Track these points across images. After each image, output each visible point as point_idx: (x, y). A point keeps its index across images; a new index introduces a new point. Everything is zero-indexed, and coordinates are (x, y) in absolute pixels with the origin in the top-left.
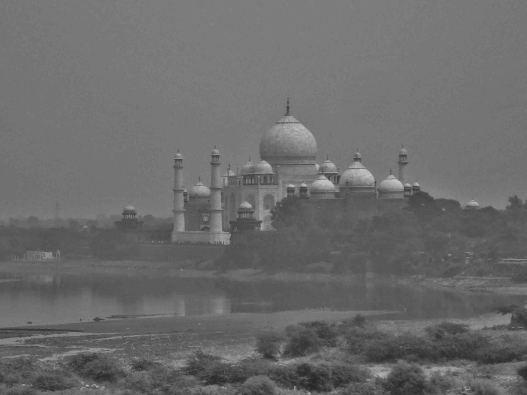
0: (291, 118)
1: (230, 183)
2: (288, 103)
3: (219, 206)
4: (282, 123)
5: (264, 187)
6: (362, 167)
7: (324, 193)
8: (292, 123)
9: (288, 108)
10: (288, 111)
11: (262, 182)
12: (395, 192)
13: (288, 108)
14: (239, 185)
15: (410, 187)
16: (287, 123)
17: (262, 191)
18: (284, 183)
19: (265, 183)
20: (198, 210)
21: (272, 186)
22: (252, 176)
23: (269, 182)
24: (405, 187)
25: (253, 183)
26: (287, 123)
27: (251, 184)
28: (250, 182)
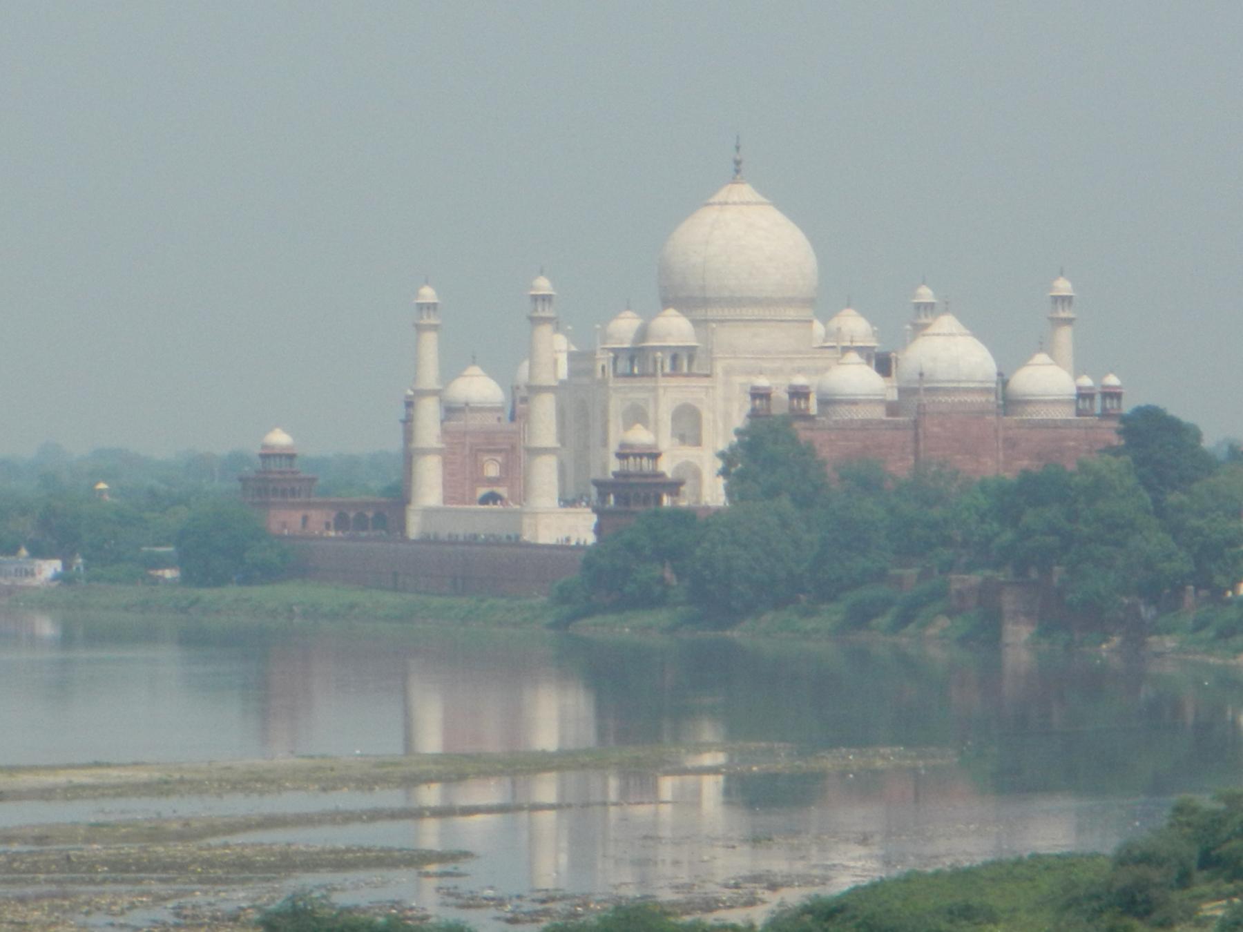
0: (745, 191)
1: (572, 372)
2: (738, 148)
4: (720, 204)
5: (674, 382)
6: (964, 330)
7: (854, 403)
8: (748, 203)
11: (667, 370)
12: (1046, 402)
13: (738, 163)
14: (599, 375)
15: (1090, 388)
16: (735, 203)
17: (671, 394)
18: (728, 372)
19: (675, 371)
21: (694, 382)
23: (685, 369)
24: (1079, 388)
25: (636, 370)
26: (735, 203)
27: (631, 375)
28: (628, 371)
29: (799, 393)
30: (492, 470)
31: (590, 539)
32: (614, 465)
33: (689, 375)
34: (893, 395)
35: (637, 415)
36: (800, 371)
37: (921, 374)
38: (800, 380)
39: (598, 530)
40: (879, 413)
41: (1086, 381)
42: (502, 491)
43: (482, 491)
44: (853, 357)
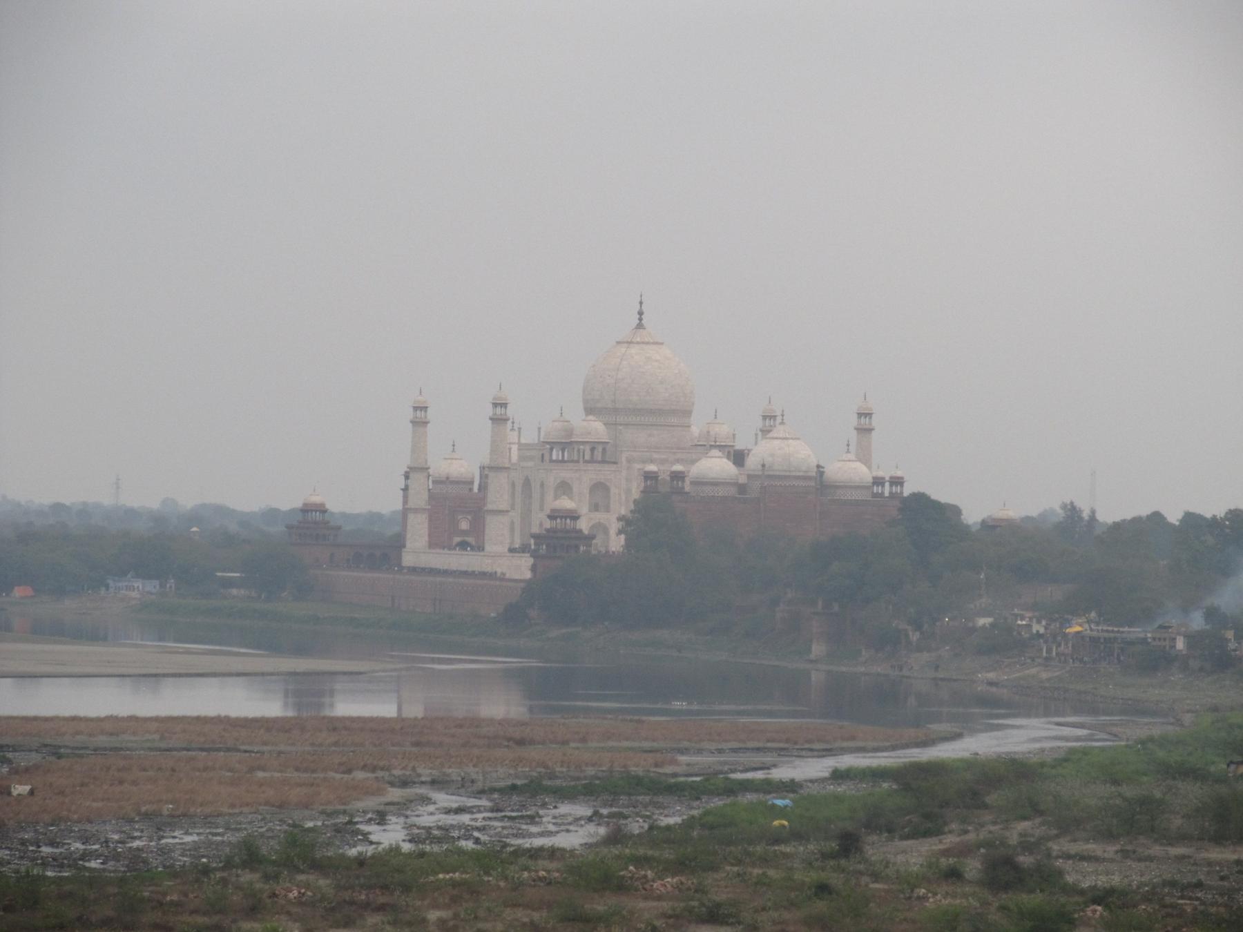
3: (498, 497)
9: (641, 313)
10: (640, 319)
13: (641, 313)
18: (629, 461)
20: (457, 509)
22: (564, 446)
29: (678, 477)
30: (464, 525)
31: (528, 575)
32: (548, 524)
33: (603, 462)
34: (743, 480)
35: (564, 488)
36: (678, 461)
37: (763, 466)
38: (678, 467)
39: (534, 569)
40: (733, 491)
41: (880, 474)
42: (470, 540)
43: (457, 539)
44: (715, 452)
